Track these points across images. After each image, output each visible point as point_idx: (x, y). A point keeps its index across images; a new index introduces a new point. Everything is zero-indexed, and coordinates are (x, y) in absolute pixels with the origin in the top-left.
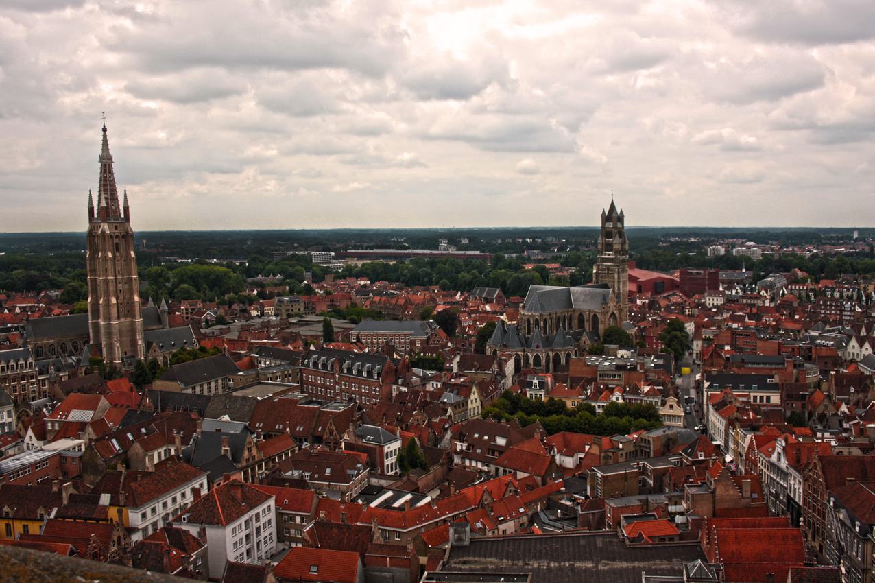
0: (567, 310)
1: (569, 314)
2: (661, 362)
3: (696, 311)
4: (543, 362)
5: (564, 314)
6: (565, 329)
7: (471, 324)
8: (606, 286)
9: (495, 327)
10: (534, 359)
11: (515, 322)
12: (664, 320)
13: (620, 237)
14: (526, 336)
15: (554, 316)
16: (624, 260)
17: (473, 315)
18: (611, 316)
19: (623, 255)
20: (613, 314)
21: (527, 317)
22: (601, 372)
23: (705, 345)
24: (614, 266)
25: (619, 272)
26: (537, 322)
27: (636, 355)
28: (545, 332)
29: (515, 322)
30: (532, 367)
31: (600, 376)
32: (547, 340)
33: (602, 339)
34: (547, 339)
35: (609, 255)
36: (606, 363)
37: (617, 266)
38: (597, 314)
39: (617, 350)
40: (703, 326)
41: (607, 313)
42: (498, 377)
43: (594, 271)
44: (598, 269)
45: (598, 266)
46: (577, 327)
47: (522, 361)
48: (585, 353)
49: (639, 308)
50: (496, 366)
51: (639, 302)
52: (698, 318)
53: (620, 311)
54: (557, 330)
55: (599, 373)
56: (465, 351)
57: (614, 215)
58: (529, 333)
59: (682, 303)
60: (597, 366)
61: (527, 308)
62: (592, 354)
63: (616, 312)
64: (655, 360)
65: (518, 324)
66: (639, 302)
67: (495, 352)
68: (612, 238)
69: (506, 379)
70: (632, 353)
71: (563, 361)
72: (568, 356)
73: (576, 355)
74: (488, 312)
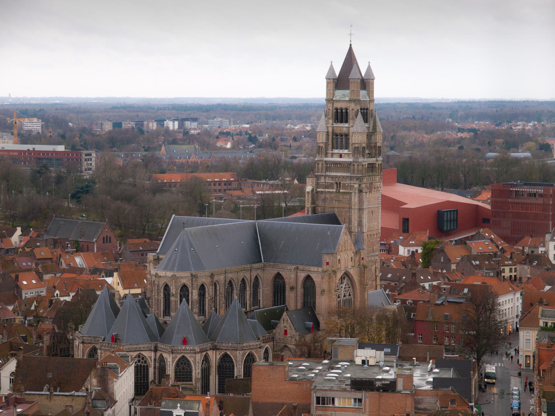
0: (249, 266)
1: (254, 274)
2: (449, 374)
3: (525, 271)
4: (196, 372)
5: (241, 275)
6: (244, 305)
7: (44, 294)
8: (333, 219)
9: (94, 301)
10: (177, 365)
11: (139, 291)
12: (455, 289)
13: (366, 120)
14: (161, 320)
15: (222, 277)
16: (372, 167)
17: (47, 277)
18: (342, 278)
19: (370, 155)
20: (347, 274)
21: (162, 282)
22: (320, 394)
23: (546, 341)
24: (351, 178)
25: (360, 191)
26: (184, 291)
27: (394, 358)
28: (202, 311)
29: (139, 291)
30: (172, 381)
31: (318, 403)
32: (205, 328)
33: (322, 325)
34: (205, 326)
35: (341, 156)
36: (332, 375)
37: (358, 179)
38: (313, 276)
39: (354, 348)
40: (541, 302)
41: (335, 272)
42: (99, 404)
43: (309, 188)
44: (318, 185)
45: (318, 177)
46: (270, 302)
47: (151, 370)
48: (286, 353)
49: (404, 264)
50: (94, 381)
51: (403, 251)
52: (530, 286)
53: (363, 269)
54: (227, 306)
55: (314, 396)
56: (29, 349)
57: (353, 75)
58: (167, 312)
59: (495, 255)
60: (310, 381)
61: (163, 263)
62: (301, 356)
63: (353, 273)
64: (437, 370)
65: (144, 293)
66: (403, 251)
67: (93, 352)
68: (347, 122)
69: (117, 407)
70: (386, 354)
71: (239, 371)
72: (250, 360)
73: (266, 358)
74: (81, 271)
